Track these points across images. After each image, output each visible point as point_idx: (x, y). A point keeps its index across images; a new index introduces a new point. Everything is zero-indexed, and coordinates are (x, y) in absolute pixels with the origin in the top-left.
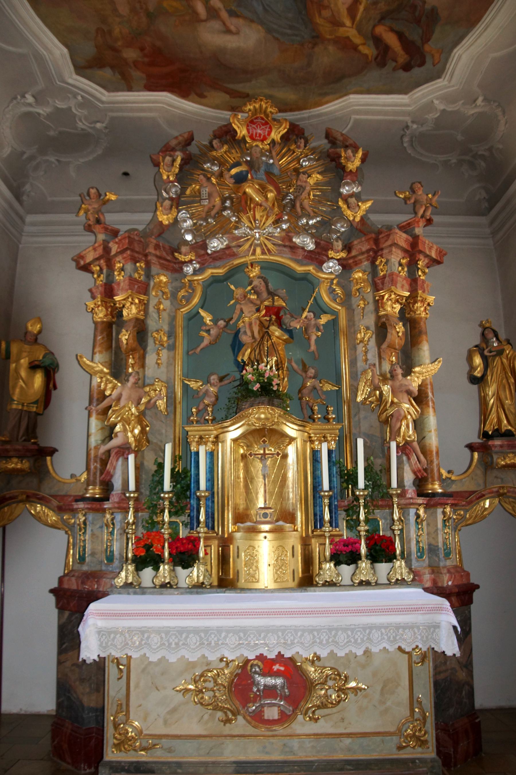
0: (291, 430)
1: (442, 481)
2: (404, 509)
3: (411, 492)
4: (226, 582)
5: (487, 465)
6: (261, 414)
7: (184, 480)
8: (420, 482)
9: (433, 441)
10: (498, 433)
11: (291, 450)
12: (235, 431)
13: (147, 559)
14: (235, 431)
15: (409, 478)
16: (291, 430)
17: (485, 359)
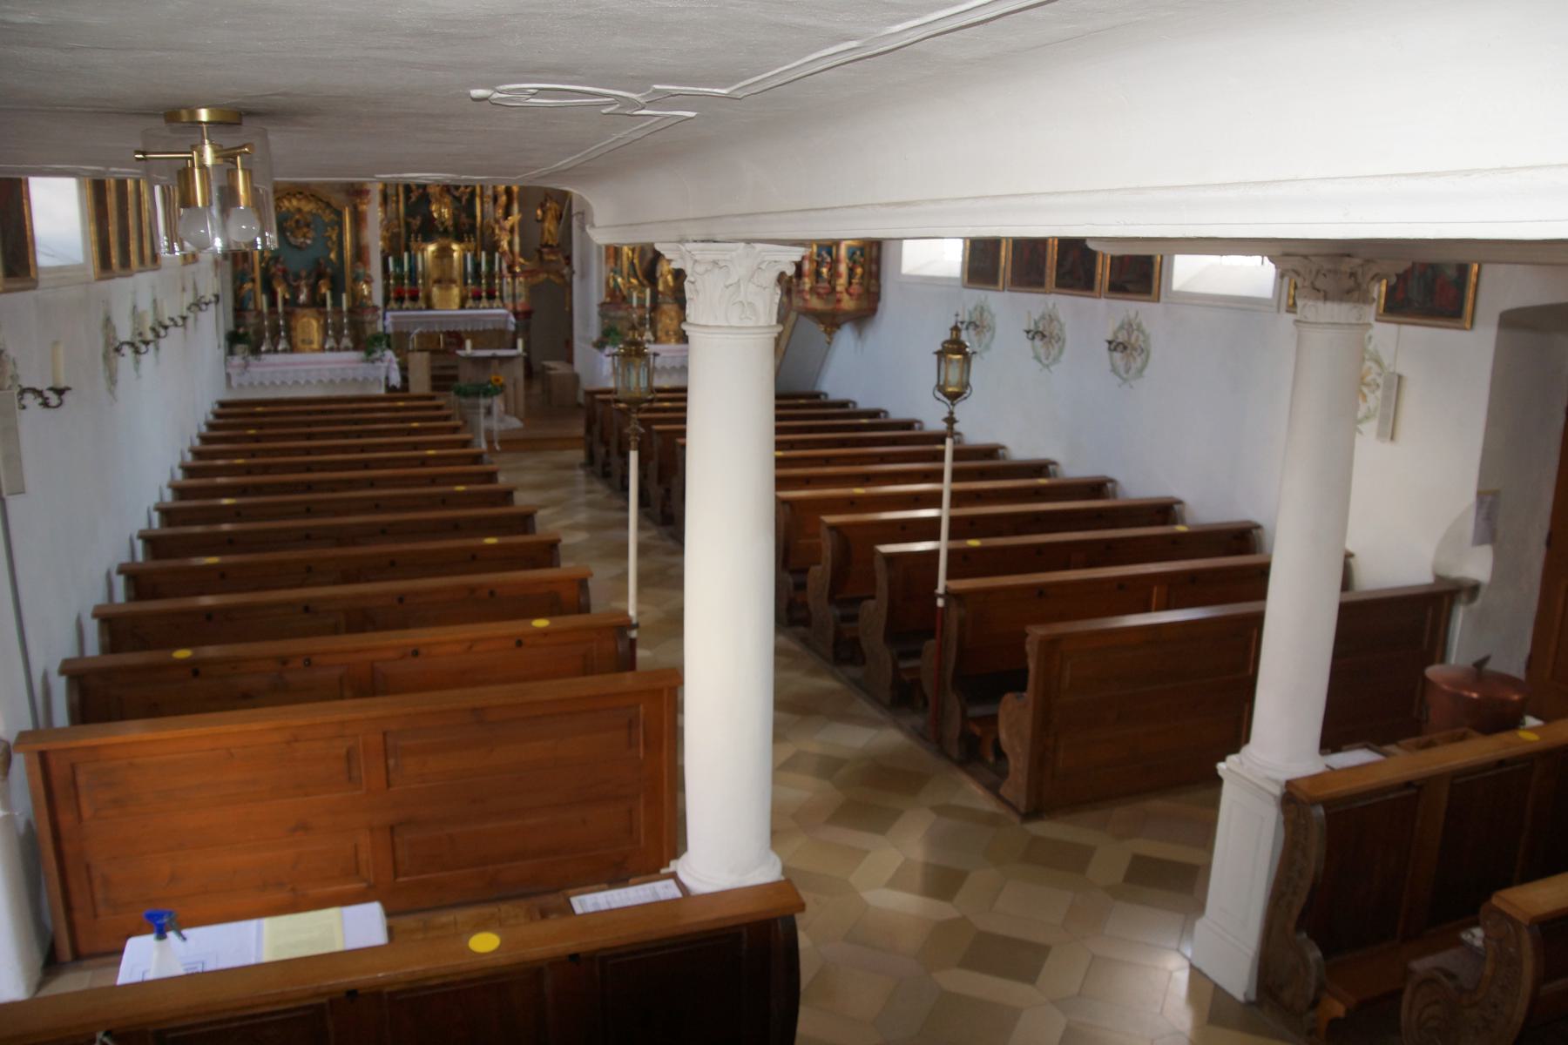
0: (455, 247)
1: (521, 265)
2: (501, 278)
3: (505, 271)
4: (429, 307)
5: (541, 259)
6: (444, 242)
7: (413, 268)
8: (510, 268)
9: (517, 248)
10: (546, 245)
11: (455, 255)
12: (431, 248)
13: (400, 299)
14: (431, 248)
15: (504, 265)
16: (455, 247)
17: (544, 213)
